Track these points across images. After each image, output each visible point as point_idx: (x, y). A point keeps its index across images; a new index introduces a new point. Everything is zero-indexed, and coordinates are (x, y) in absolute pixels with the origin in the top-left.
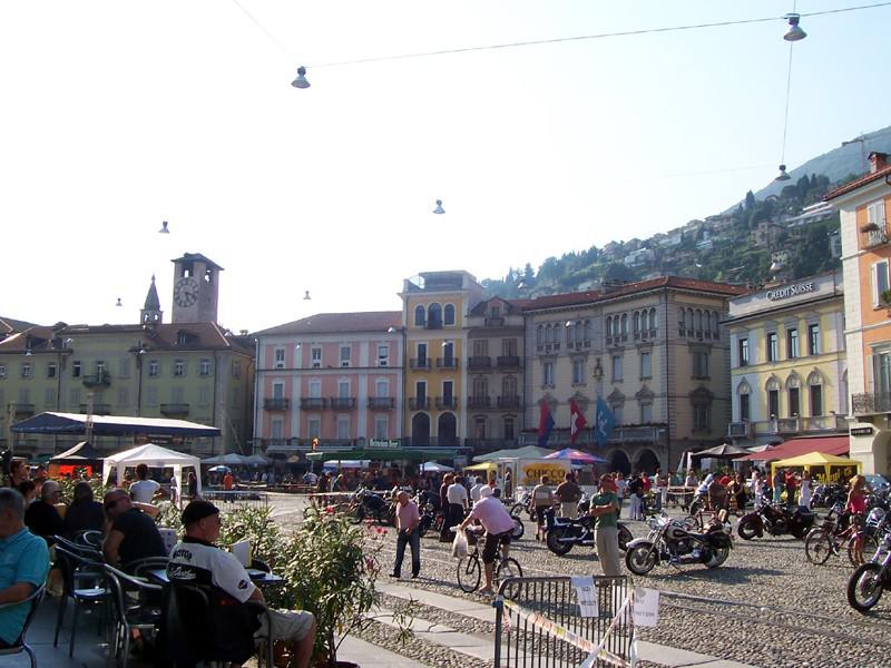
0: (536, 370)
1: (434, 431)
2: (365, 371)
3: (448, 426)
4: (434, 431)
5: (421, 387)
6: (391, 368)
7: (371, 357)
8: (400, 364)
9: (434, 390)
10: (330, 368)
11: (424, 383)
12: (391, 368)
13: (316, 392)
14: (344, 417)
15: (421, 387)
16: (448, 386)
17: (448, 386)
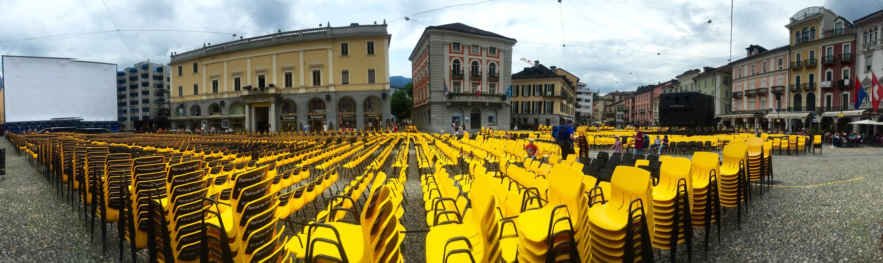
0: (862, 61)
1: (804, 104)
2: (773, 74)
3: (811, 99)
4: (804, 104)
5: (798, 79)
6: (784, 70)
7: (775, 67)
8: (788, 68)
9: (805, 79)
10: (758, 74)
11: (799, 76)
12: (784, 70)
13: (753, 87)
14: (763, 99)
15: (798, 79)
16: (812, 77)
17: (812, 77)
